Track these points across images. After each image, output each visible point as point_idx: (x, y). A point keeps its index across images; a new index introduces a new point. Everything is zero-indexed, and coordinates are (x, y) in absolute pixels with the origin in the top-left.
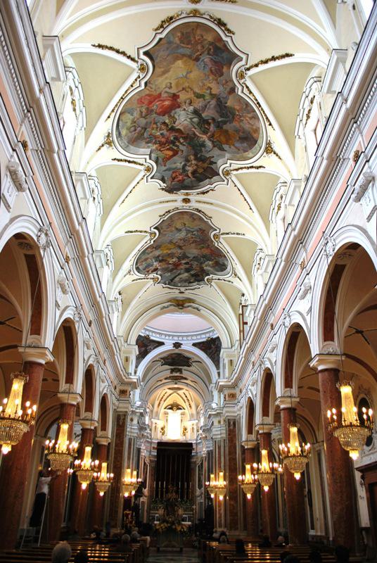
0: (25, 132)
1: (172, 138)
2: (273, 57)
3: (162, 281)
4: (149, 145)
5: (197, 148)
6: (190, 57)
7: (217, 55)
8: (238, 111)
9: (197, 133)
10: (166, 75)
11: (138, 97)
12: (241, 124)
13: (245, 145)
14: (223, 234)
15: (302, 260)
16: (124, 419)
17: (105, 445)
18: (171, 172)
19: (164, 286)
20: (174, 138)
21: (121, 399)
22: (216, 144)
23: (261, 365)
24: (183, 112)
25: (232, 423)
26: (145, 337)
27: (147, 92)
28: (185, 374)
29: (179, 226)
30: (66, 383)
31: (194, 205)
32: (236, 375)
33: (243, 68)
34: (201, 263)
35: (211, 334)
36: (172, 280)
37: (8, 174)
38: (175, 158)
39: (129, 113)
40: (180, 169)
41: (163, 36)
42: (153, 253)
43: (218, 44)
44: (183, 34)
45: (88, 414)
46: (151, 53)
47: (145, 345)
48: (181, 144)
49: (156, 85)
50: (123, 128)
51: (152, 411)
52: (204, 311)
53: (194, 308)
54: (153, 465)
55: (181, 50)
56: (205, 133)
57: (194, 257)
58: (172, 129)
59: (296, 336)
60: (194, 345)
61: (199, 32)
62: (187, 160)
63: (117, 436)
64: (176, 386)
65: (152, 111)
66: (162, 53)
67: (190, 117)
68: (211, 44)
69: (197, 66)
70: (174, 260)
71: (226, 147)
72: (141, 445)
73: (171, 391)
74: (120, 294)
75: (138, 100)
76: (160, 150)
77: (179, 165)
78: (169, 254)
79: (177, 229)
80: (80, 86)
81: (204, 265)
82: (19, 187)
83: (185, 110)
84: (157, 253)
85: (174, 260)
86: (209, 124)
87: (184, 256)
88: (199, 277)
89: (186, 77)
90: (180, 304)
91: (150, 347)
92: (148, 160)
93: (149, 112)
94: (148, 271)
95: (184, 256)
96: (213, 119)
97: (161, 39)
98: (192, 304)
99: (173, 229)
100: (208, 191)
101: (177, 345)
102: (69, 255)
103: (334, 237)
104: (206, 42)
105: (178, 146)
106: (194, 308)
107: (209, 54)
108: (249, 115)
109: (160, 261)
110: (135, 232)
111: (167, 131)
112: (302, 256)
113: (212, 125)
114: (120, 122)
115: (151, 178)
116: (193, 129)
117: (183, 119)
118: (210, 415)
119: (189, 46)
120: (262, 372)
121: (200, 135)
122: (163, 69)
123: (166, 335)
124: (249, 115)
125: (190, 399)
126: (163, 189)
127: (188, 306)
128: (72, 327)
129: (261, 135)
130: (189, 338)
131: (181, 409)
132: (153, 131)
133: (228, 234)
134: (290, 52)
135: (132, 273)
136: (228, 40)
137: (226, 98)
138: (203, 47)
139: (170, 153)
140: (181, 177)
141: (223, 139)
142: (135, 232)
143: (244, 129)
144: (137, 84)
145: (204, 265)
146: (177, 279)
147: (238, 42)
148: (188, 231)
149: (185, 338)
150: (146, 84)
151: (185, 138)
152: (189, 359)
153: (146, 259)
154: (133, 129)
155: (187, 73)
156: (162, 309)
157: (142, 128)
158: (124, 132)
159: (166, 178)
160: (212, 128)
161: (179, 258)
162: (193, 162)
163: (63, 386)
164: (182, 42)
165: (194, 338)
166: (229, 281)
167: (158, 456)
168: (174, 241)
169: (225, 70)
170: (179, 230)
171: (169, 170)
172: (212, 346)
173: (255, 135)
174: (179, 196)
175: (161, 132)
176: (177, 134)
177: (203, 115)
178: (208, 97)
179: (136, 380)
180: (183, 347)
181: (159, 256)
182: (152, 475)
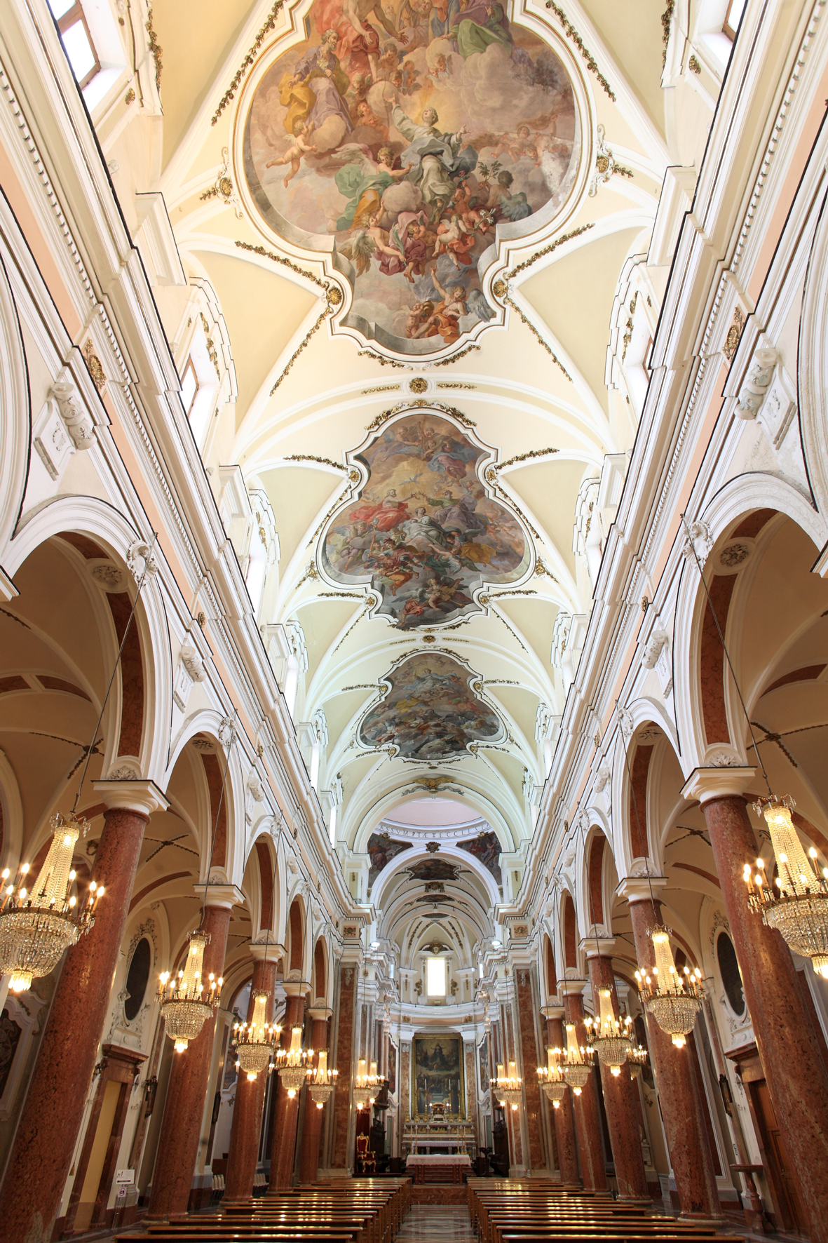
0: (202, 603)
1: (402, 559)
2: (531, 452)
3: (402, 753)
4: (370, 569)
5: (439, 570)
6: (418, 456)
7: (455, 452)
8: (491, 519)
9: (437, 550)
10: (387, 481)
11: (350, 512)
12: (498, 535)
13: (506, 562)
14: (486, 682)
15: (595, 734)
16: (352, 976)
17: (323, 1021)
18: (404, 603)
19: (406, 759)
20: (405, 558)
21: (346, 942)
22: (464, 562)
23: (556, 884)
24: (414, 525)
25: (523, 976)
26: (381, 836)
27: (363, 504)
28: (449, 890)
29: (421, 674)
30: (262, 928)
31: (440, 643)
32: (524, 897)
33: (492, 467)
34: (460, 724)
35: (485, 827)
36: (417, 751)
37: (182, 663)
38: (409, 583)
39: (338, 532)
40: (416, 597)
41: (379, 434)
42: (386, 714)
43: (456, 439)
44: (406, 429)
45: (296, 972)
46: (364, 456)
47: (381, 849)
48: (416, 565)
49: (374, 495)
50: (331, 552)
51: (399, 955)
52: (469, 794)
53: (454, 790)
55: (405, 449)
56: (448, 548)
57: (447, 717)
58: (401, 547)
59: (598, 845)
60: (460, 845)
61: (427, 425)
62: (426, 586)
63: (341, 1004)
64: (435, 911)
65: (372, 526)
66: (380, 455)
67: (425, 529)
68: (446, 438)
69: (429, 466)
70: (417, 722)
71: (479, 566)
72: (383, 1016)
73: (429, 920)
74: (339, 777)
75: (350, 515)
76: (386, 575)
77: (415, 593)
78: (410, 713)
79: (419, 678)
80: (269, 509)
81: (463, 727)
82: (195, 677)
83: (416, 521)
84: (392, 713)
85: (417, 722)
86: (453, 537)
87: (433, 715)
88: (457, 744)
89: (415, 481)
90: (432, 785)
91: (389, 852)
92: (370, 590)
93: (367, 528)
94: (380, 741)
95: (433, 715)
96: (458, 531)
97: (376, 439)
98: (450, 784)
99: (413, 678)
100: (460, 625)
101: (433, 847)
102: (262, 744)
103: (630, 709)
104: (439, 436)
105: (411, 569)
106: (454, 790)
107: (443, 451)
108: (509, 525)
109: (397, 725)
110: (356, 687)
111: (395, 550)
112: (595, 728)
113: (457, 539)
114: (327, 546)
115: (376, 613)
116: (431, 545)
117: (415, 533)
118: (491, 961)
119: (417, 443)
120: (559, 896)
121: (442, 552)
122: (382, 475)
123: (414, 832)
124: (509, 525)
125: (460, 934)
126: (394, 626)
127: (445, 788)
128: (269, 844)
129: (526, 550)
130: (451, 834)
131: (446, 949)
132: (374, 552)
133: (494, 682)
134: (553, 447)
135: (355, 745)
136: (469, 432)
137: (474, 504)
138: (435, 443)
139: (401, 578)
140: (419, 607)
141: (475, 556)
142: (356, 687)
143: (501, 542)
144: (348, 495)
145: (463, 727)
146: (424, 749)
147: (482, 435)
148: (436, 681)
149: (444, 835)
150: (360, 494)
151: (420, 557)
152: (452, 867)
153: (377, 723)
154: (345, 552)
155: (416, 477)
156: (404, 794)
157: (359, 550)
158: (333, 558)
159: (397, 611)
160: (457, 541)
161: (425, 719)
162: (435, 587)
163: (258, 933)
164: (405, 439)
165: (459, 833)
166: (503, 750)
168: (416, 695)
169: (467, 469)
170: (422, 680)
171: (401, 599)
172: (488, 846)
173: (518, 550)
174: (419, 633)
175: (386, 552)
176: (408, 553)
177: (444, 526)
178: (447, 504)
179: (368, 911)
180: (442, 850)
181: (394, 718)
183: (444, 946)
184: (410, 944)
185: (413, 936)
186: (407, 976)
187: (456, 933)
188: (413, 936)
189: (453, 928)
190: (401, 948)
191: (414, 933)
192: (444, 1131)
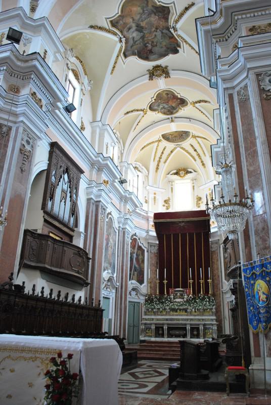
54: (155, 250)
73: (170, 146)
131: (191, 172)
167: (159, 236)
182: (152, 265)
183: (189, 170)
184: (157, 168)
185: (159, 161)
186: (155, 194)
187: (199, 155)
188: (159, 161)
189: (195, 150)
190: (148, 171)
191: (160, 158)
192: (184, 313)
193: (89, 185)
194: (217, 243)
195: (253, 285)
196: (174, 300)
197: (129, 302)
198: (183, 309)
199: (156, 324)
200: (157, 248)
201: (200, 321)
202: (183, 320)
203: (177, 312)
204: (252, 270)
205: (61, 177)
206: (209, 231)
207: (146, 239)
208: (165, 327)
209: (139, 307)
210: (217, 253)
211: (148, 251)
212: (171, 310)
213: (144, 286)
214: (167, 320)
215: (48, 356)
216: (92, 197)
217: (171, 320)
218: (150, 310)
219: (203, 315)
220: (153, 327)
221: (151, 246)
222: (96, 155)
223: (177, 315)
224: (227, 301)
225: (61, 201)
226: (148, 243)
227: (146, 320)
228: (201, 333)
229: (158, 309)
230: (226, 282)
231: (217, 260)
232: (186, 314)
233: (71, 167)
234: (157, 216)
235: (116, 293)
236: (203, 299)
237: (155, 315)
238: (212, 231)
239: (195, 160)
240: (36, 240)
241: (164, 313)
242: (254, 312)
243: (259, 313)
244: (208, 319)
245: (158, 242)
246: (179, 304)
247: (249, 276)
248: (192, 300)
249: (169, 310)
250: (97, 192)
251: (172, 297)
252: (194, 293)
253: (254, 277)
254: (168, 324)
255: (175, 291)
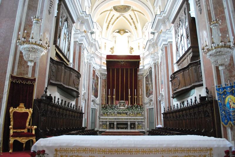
54: (105, 77)
73: (117, 14)
131: (127, 32)
167: (108, 70)
182: (103, 86)
183: (126, 31)
184: (108, 28)
185: (109, 23)
186: (105, 43)
187: (134, 22)
188: (109, 23)
189: (132, 19)
191: (110, 21)
192: (125, 115)
193: (75, 32)
194: (142, 75)
195: (224, 99)
196: (120, 108)
197: (92, 108)
198: (125, 113)
199: (109, 122)
200: (105, 76)
201: (135, 120)
202: (125, 119)
203: (121, 114)
204: (224, 90)
205: (64, 24)
206: (138, 67)
207: (99, 71)
208: (115, 123)
209: (95, 111)
210: (142, 81)
211: (100, 78)
212: (118, 113)
213: (98, 99)
214: (115, 119)
215: (200, 154)
216: (78, 40)
217: (118, 119)
218: (105, 113)
219: (136, 116)
220: (108, 123)
221: (102, 75)
222: (82, 12)
223: (121, 116)
224: (147, 108)
225: (64, 40)
226: (101, 73)
227: (103, 119)
228: (136, 126)
229: (110, 112)
230: (147, 98)
231: (142, 85)
232: (127, 115)
233: (69, 18)
234: (108, 57)
235: (85, 103)
236: (137, 107)
237: (108, 116)
238: (140, 68)
239: (131, 25)
240: (55, 65)
241: (114, 115)
242: (225, 114)
243: (230, 115)
244: (140, 118)
245: (106, 73)
246: (123, 110)
247: (221, 93)
248: (131, 107)
249: (116, 113)
250: (81, 37)
251: (118, 105)
252: (131, 103)
253: (225, 94)
254: (117, 122)
255: (120, 102)
